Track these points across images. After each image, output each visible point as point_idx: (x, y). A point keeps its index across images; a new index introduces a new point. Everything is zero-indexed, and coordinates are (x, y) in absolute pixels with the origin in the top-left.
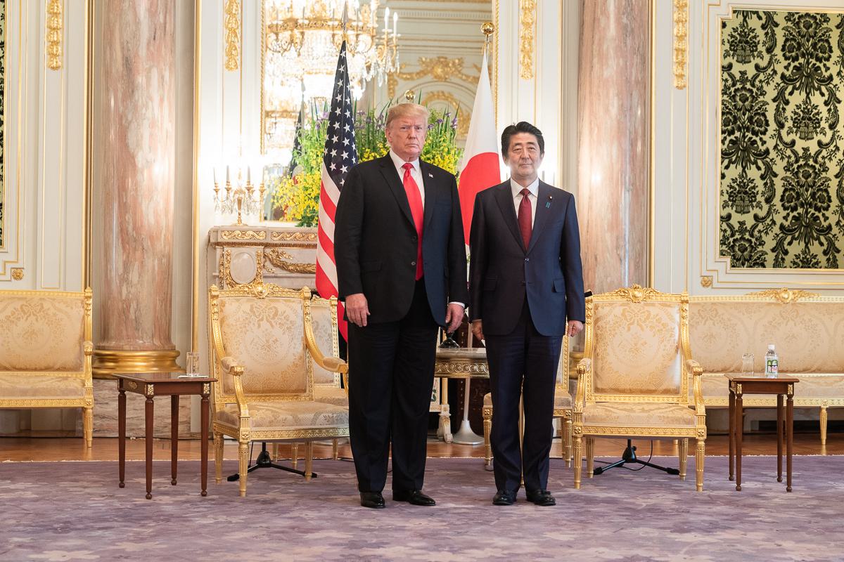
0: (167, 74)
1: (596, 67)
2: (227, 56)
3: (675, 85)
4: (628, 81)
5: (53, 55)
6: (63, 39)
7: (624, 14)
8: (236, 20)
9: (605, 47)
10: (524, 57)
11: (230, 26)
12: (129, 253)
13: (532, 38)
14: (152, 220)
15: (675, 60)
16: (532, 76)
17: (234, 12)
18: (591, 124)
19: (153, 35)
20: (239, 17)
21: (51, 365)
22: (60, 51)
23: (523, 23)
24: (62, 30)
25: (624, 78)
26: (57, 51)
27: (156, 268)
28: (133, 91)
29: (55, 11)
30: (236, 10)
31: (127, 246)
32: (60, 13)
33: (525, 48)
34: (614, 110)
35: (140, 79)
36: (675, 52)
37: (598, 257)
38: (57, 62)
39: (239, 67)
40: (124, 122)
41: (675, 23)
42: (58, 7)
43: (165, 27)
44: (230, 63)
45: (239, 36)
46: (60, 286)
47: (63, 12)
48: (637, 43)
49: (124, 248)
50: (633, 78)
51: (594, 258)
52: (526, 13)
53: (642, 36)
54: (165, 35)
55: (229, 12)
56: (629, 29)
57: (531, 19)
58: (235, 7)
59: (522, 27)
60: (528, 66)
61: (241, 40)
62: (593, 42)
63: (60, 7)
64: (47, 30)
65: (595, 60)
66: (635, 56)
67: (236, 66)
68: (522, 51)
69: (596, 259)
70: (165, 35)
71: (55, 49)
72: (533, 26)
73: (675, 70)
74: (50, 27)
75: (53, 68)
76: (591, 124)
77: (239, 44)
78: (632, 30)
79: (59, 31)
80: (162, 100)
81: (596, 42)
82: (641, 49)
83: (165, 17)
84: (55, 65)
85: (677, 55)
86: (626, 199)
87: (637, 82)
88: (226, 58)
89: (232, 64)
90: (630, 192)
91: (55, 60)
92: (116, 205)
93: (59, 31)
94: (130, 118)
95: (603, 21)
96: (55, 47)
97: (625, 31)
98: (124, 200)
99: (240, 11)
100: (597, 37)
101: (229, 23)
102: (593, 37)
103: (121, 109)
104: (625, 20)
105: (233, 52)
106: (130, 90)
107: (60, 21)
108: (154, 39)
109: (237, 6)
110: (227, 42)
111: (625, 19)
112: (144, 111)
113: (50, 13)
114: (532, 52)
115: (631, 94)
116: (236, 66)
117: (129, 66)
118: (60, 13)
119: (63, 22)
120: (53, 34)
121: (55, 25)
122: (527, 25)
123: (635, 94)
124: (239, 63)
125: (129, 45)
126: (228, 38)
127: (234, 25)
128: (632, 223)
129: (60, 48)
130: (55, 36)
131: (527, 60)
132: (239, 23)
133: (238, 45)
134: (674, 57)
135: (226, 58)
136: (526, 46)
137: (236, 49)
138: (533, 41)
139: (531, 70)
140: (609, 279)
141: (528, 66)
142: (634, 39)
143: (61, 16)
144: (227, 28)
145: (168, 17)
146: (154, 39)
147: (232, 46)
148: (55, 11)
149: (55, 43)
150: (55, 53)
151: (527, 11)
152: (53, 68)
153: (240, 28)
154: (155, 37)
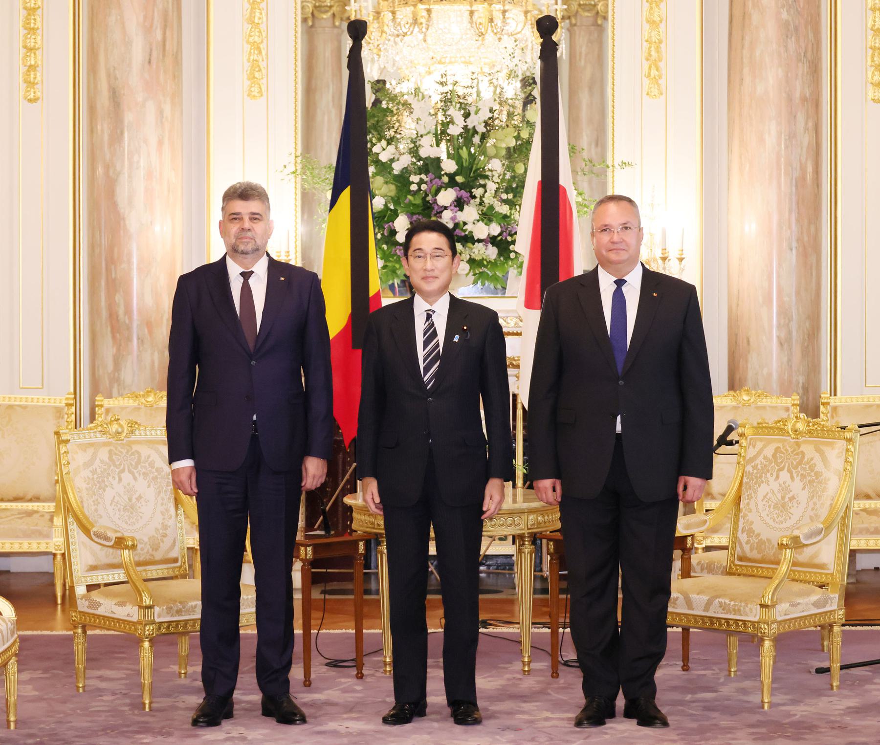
0: (167, 108)
1: (747, 79)
2: (249, 79)
3: (870, 95)
4: (790, 99)
5: (30, 84)
6: (42, 61)
7: (783, 6)
8: (260, 32)
9: (758, 53)
10: (650, 69)
11: (251, 40)
12: (120, 345)
13: (660, 42)
14: (149, 300)
15: (869, 63)
16: (662, 94)
17: (256, 21)
18: (741, 158)
19: (147, 60)
20: (263, 27)
21: (21, 495)
22: (39, 78)
23: (648, 22)
24: (40, 50)
25: (784, 95)
26: (35, 78)
27: (156, 364)
28: (122, 133)
29: (32, 25)
30: (260, 18)
31: (118, 335)
32: (38, 28)
33: (650, 55)
34: (771, 139)
35: (129, 117)
36: (870, 52)
37: (751, 340)
38: (35, 93)
39: (264, 93)
40: (111, 173)
41: (870, 12)
42: (35, 19)
43: (164, 45)
44: (253, 89)
45: (264, 52)
46: (43, 385)
47: (42, 25)
48: (803, 45)
49: (114, 337)
50: (798, 95)
51: (745, 341)
52: (651, 8)
53: (811, 36)
54: (164, 56)
55: (251, 21)
56: (792, 27)
57: (659, 16)
58: (257, 14)
59: (647, 27)
60: (656, 81)
61: (267, 58)
62: (743, 47)
63: (38, 19)
64: (23, 51)
65: (746, 70)
66: (800, 64)
67: (260, 92)
68: (647, 60)
69: (748, 342)
70: (164, 56)
71: (32, 76)
72: (663, 25)
73: (870, 76)
74: (25, 47)
75: (30, 101)
76: (741, 158)
77: (265, 63)
78: (796, 29)
79: (37, 52)
80: (160, 143)
81: (747, 43)
82: (809, 54)
83: (164, 34)
84: (32, 96)
85: (873, 56)
86: (792, 258)
87: (804, 99)
88: (249, 83)
89: (255, 89)
90: (794, 251)
91: (32, 90)
92: (103, 283)
93: (37, 52)
94: (118, 168)
95: (755, 18)
96: (32, 73)
97: (787, 30)
98: (113, 276)
99: (265, 20)
100: (747, 39)
101: (251, 36)
102: (743, 39)
103: (108, 157)
104: (785, 15)
105: (257, 75)
106: (119, 131)
107: (39, 38)
108: (150, 62)
109: (261, 14)
110: (249, 60)
111: (785, 13)
112: (136, 158)
113: (26, 29)
114: (660, 60)
115: (795, 116)
116: (260, 92)
117: (115, 96)
118: (38, 28)
119: (42, 39)
120: (30, 56)
121: (33, 44)
122: (652, 23)
123: (801, 118)
124: (264, 88)
125: (117, 72)
126: (249, 56)
127: (256, 39)
128: (798, 293)
129: (38, 74)
130: (33, 59)
131: (654, 72)
132: (264, 35)
133: (262, 65)
134: (869, 59)
135: (247, 83)
136: (653, 53)
137: (260, 70)
138: (663, 46)
139: (659, 85)
140: (765, 371)
141: (656, 81)
142: (798, 41)
143: (39, 31)
144: (248, 42)
145: (168, 33)
146: (150, 62)
147: (255, 66)
148: (32, 25)
149: (32, 68)
150: (32, 80)
151: (654, 5)
152: (30, 101)
153: (265, 41)
154: (150, 59)
